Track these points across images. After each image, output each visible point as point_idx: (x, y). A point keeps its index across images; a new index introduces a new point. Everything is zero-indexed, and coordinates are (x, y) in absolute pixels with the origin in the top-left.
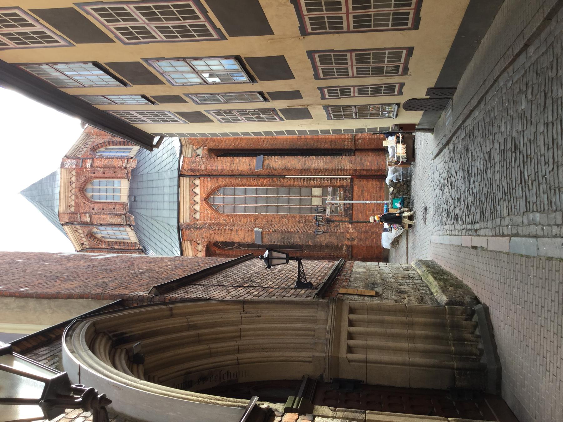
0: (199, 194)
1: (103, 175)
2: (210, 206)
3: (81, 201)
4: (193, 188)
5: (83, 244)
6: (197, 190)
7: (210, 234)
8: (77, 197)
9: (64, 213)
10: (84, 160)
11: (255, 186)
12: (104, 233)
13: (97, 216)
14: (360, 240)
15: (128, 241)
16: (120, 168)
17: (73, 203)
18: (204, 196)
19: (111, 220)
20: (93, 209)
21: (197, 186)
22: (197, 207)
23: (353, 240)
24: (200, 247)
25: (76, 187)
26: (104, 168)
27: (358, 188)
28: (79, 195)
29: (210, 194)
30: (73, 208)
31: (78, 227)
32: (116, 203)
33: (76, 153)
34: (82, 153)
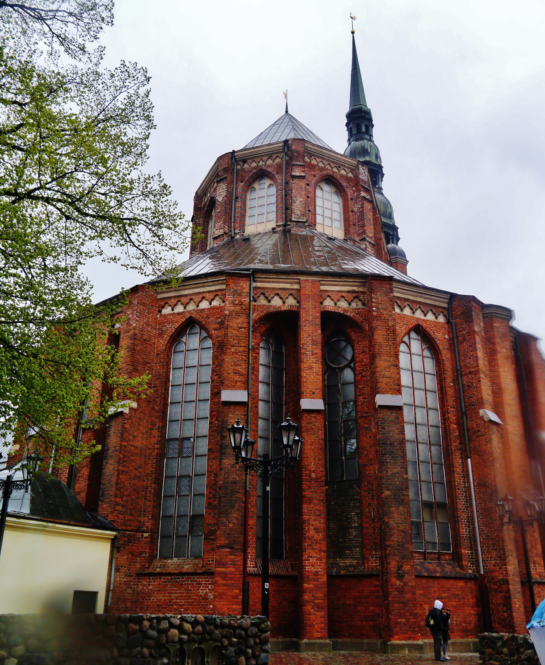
1: (350, 210)
5: (245, 161)
14: (401, 591)
17: (314, 162)
19: (298, 202)
20: (308, 185)
25: (334, 172)
28: (324, 172)
30: (309, 161)
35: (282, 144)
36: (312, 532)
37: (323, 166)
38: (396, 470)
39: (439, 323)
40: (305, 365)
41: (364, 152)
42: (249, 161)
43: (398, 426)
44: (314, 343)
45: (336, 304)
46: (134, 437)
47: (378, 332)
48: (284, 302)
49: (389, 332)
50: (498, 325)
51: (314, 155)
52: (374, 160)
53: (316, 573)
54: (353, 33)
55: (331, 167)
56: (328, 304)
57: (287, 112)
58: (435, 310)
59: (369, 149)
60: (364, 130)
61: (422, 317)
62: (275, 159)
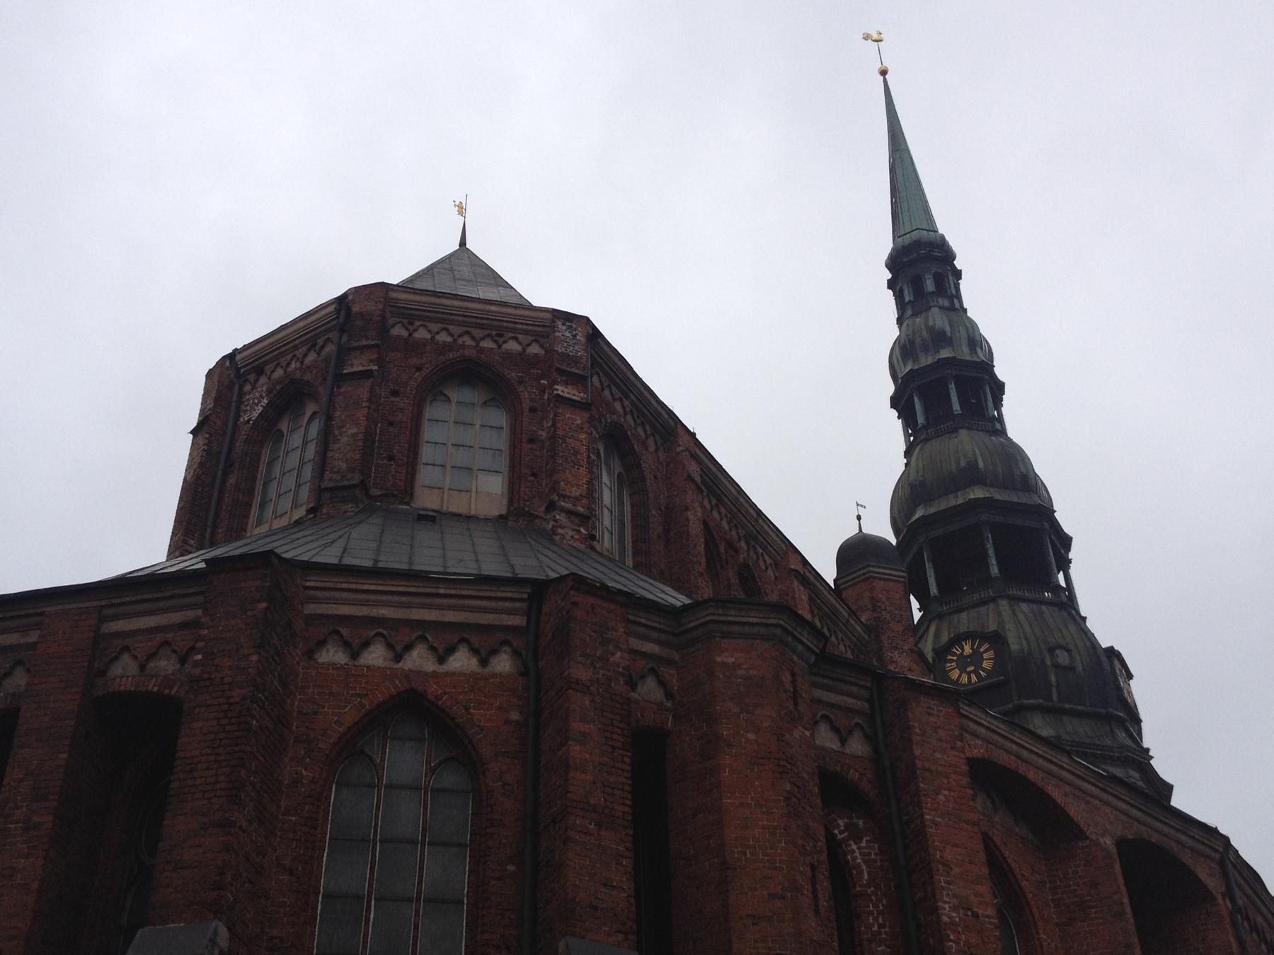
4: (475, 640)
5: (259, 371)
6: (462, 661)
10: (578, 380)
12: (296, 439)
13: (365, 396)
15: (252, 520)
16: (554, 488)
17: (422, 334)
18: (433, 689)
19: (344, 440)
20: (395, 393)
22: (376, 656)
24: (166, 665)
25: (482, 350)
26: (553, 437)
30: (405, 334)
31: (330, 349)
33: (607, 374)
34: (607, 392)
35: (331, 308)
37: (449, 339)
39: (494, 675)
41: (940, 339)
42: (268, 368)
45: (142, 668)
49: (225, 721)
50: (731, 660)
51: (420, 318)
52: (965, 354)
54: (884, 73)
55: (473, 338)
56: (124, 672)
57: (463, 243)
58: (485, 642)
59: (948, 329)
60: (930, 286)
61: (430, 666)
62: (323, 347)
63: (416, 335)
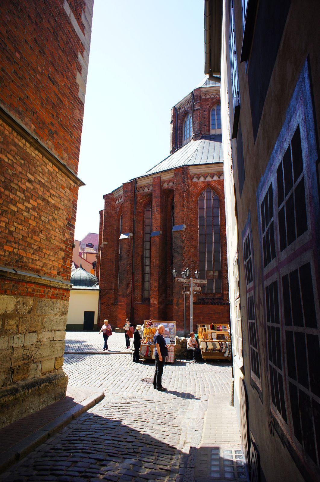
0: (212, 180)
2: (203, 189)
3: (210, 102)
5: (180, 109)
7: (180, 189)
8: (212, 99)
9: (200, 91)
11: (221, 224)
12: (188, 122)
13: (198, 114)
17: (208, 97)
19: (196, 124)
20: (204, 111)
21: (219, 178)
22: (202, 179)
23: (178, 305)
24: (171, 184)
27: (222, 309)
28: (214, 100)
29: (213, 188)
30: (205, 97)
32: (209, 126)
36: (153, 288)
38: (178, 260)
40: (154, 217)
43: (180, 239)
44: (157, 206)
45: (168, 185)
46: (107, 255)
47: (176, 196)
48: (149, 189)
53: (154, 304)
56: (165, 185)
61: (210, 180)
63: (207, 97)
